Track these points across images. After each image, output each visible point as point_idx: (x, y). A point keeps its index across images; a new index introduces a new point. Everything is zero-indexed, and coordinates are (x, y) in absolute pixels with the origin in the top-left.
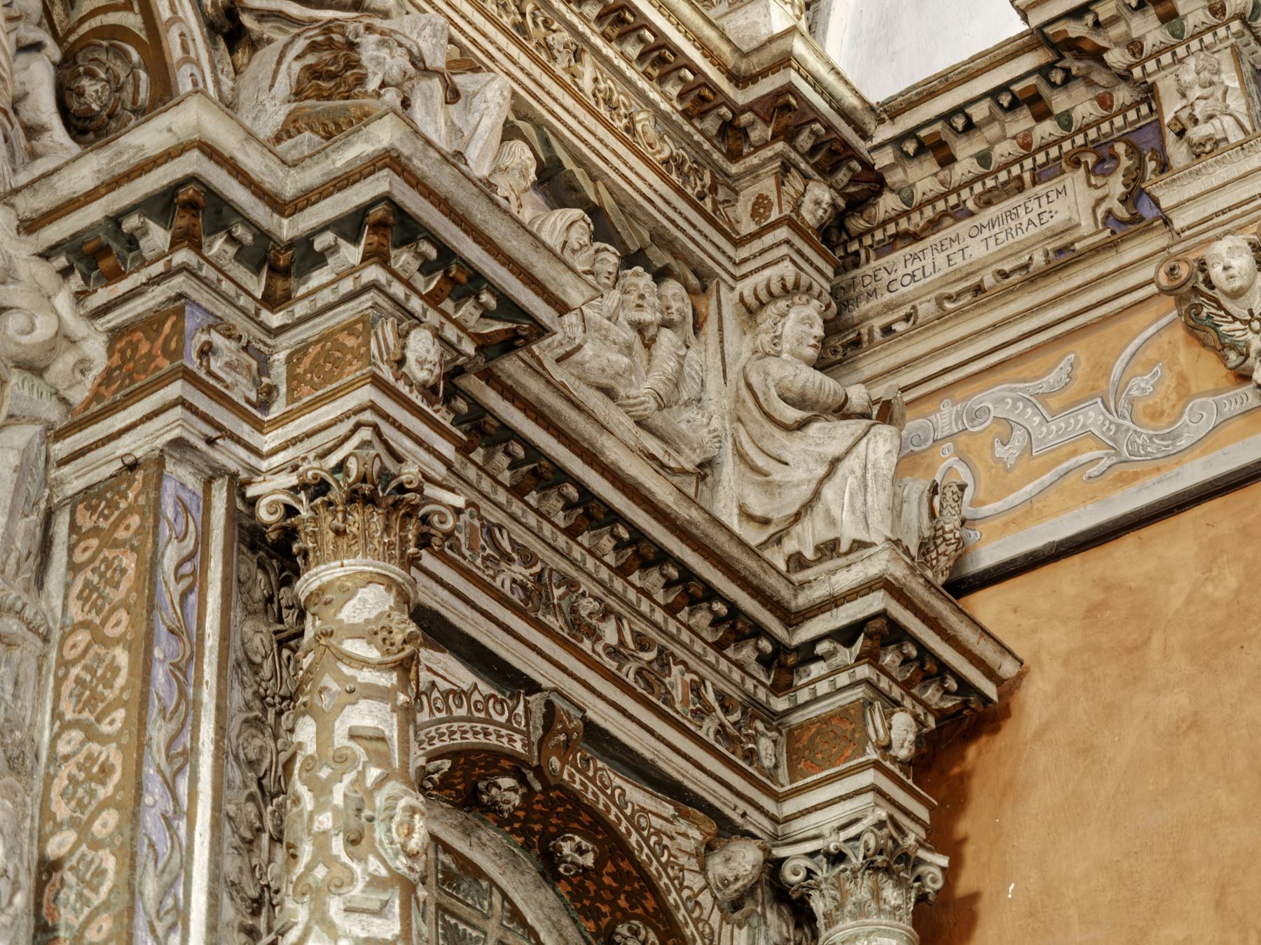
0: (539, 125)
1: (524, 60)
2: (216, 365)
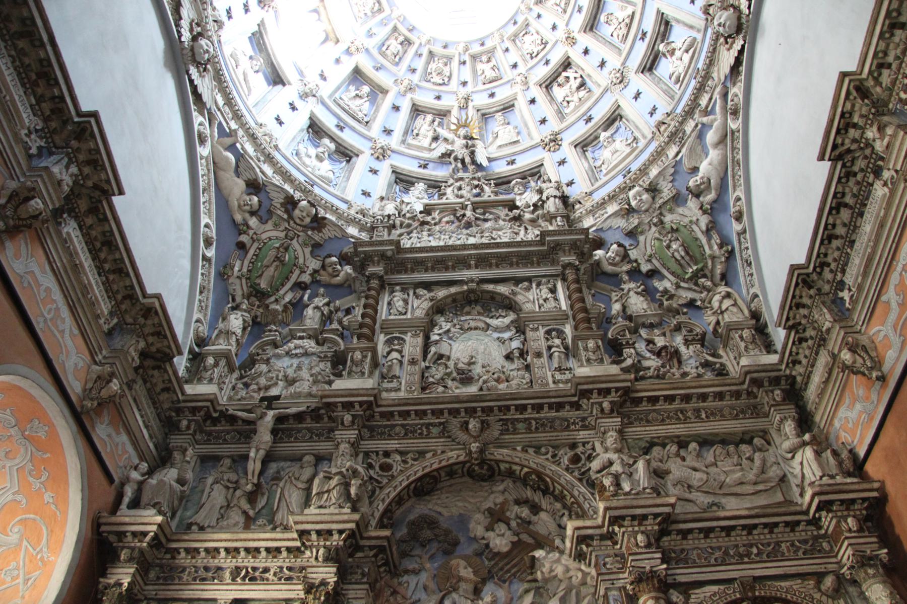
1: (682, 426)
2: (608, 566)
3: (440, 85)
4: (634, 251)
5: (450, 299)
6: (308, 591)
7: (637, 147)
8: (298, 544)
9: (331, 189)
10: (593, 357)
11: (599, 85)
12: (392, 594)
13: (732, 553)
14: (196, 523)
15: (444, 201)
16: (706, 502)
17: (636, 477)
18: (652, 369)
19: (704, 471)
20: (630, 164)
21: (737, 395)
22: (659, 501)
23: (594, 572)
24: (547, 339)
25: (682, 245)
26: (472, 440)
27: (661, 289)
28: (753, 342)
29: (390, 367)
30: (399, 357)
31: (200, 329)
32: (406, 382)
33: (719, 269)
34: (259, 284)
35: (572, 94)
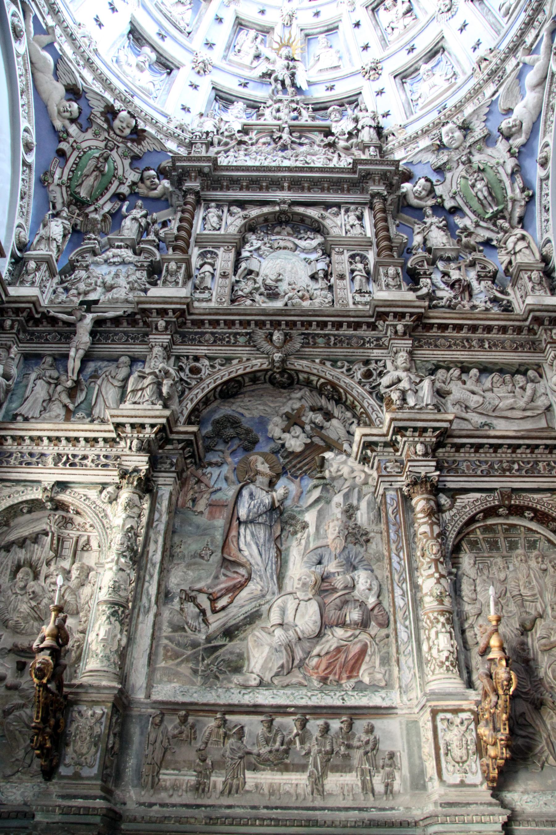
0: (477, 362)
1: (466, 353)
2: (388, 470)
4: (440, 187)
5: (262, 218)
6: (122, 477)
7: (455, 83)
8: (114, 435)
9: (151, 101)
10: (392, 283)
12: (197, 483)
13: (496, 467)
14: (21, 415)
15: (262, 121)
16: (479, 422)
17: (421, 394)
18: (445, 300)
19: (481, 395)
20: (446, 100)
21: (519, 330)
22: (439, 417)
23: (375, 474)
24: (351, 263)
25: (487, 186)
26: (275, 350)
27: (461, 226)
28: (540, 283)
29: (203, 279)
30: (212, 271)
31: (22, 234)
32: (217, 294)
33: (518, 212)
34: (79, 193)
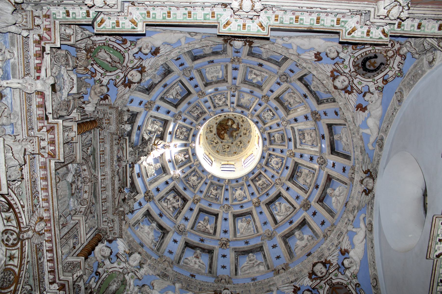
3: (176, 133)
11: (176, 219)
35: (171, 204)
